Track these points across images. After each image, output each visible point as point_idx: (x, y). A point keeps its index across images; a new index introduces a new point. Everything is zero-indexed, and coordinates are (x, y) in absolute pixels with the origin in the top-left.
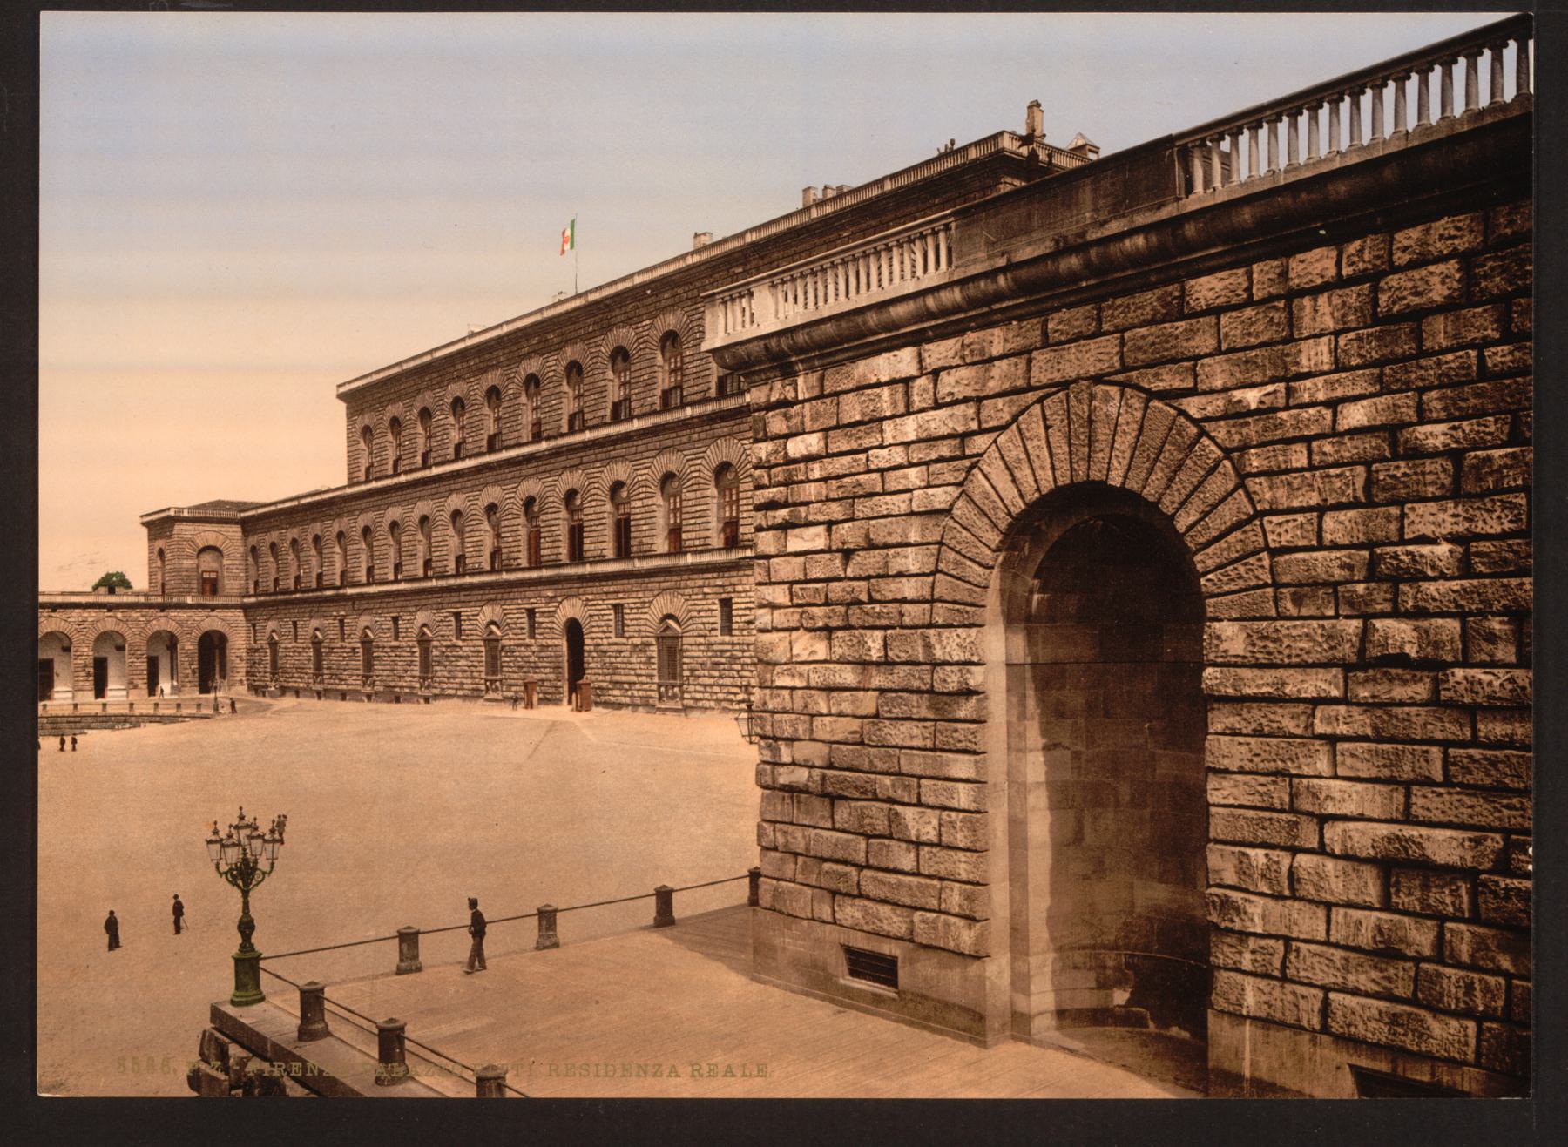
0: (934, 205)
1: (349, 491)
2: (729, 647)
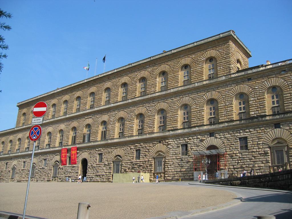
0: (209, 48)
1: (16, 129)
2: (138, 163)
